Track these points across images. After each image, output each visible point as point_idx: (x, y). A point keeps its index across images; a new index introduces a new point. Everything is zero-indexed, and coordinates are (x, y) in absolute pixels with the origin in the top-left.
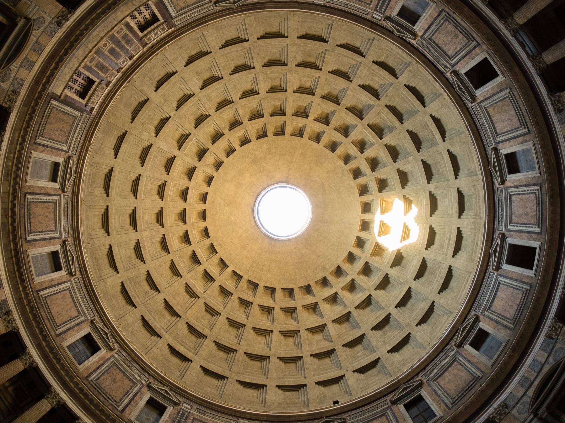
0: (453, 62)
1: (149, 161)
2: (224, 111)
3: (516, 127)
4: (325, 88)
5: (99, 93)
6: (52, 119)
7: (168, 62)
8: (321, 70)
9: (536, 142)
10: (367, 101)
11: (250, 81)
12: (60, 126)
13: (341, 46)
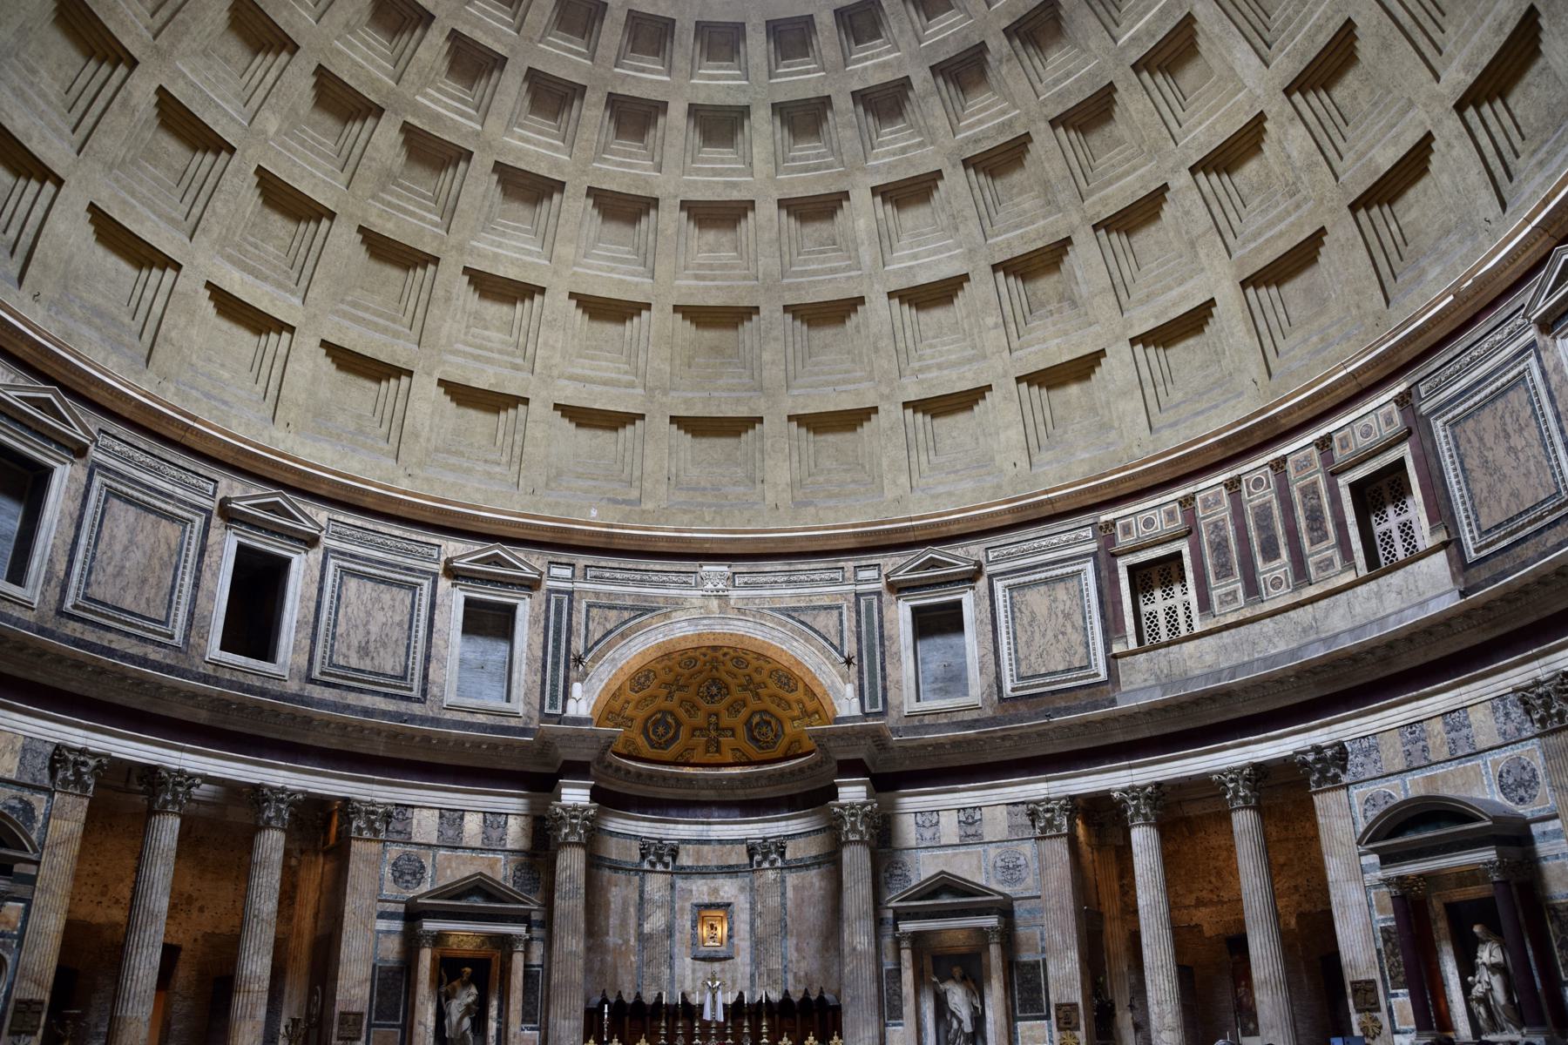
0: (332, 563)
1: (1319, 28)
2: (1001, 128)
3: (93, 577)
4: (651, 237)
5: (1358, 434)
6: (1504, 505)
7: (1149, 391)
8: (676, 308)
9: (29, 613)
10: (500, 245)
11: (905, 241)
12: (1499, 453)
13: (629, 419)
